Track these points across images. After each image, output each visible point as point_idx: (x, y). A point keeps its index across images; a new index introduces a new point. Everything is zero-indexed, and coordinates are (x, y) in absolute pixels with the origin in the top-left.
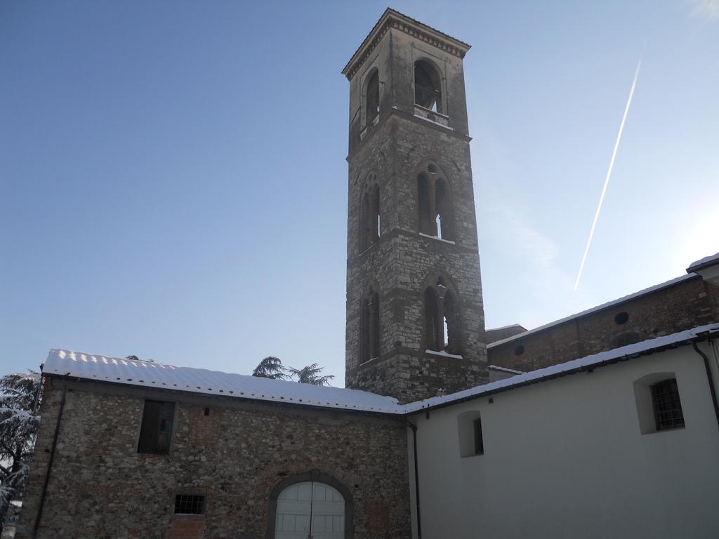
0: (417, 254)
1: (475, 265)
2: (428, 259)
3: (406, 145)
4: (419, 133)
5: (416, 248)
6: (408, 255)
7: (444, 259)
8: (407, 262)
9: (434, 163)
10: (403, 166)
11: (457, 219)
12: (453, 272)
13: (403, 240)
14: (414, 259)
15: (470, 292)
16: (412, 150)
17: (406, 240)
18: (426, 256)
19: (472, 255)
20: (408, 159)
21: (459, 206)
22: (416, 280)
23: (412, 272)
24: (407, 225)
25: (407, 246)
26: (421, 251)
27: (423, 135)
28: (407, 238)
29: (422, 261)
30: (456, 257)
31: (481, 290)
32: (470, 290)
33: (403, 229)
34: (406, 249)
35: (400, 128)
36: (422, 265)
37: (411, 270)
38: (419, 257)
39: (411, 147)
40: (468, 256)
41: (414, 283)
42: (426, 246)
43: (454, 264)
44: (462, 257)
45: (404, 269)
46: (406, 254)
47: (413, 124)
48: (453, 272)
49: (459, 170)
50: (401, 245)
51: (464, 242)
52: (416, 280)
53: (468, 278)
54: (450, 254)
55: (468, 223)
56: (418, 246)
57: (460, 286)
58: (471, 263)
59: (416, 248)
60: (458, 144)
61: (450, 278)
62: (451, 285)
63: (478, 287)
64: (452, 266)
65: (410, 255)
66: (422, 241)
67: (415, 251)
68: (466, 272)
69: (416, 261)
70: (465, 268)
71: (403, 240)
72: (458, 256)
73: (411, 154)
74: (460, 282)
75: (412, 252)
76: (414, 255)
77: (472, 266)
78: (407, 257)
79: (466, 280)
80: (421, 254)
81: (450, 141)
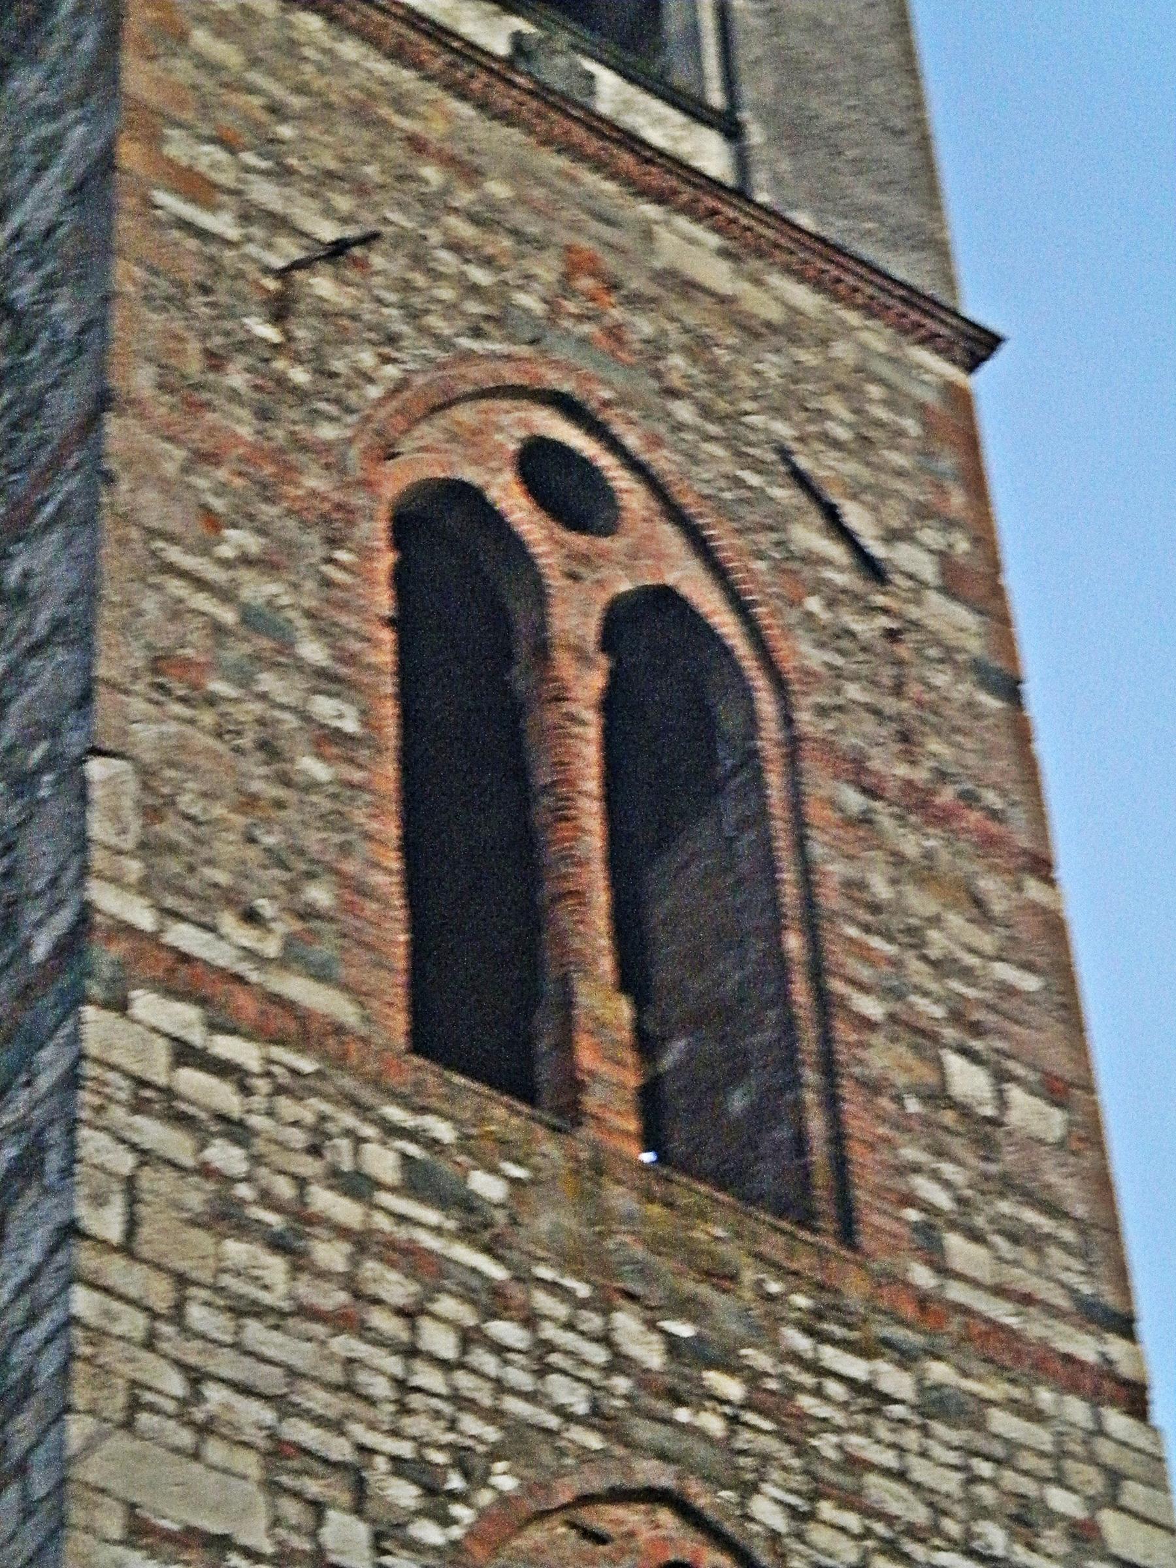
2: (505, 1331)
5: (358, 1185)
6: (244, 1228)
8: (243, 1310)
10: (215, 361)
13: (184, 1054)
16: (337, 250)
17: (223, 1069)
18: (493, 1301)
20: (280, 310)
24: (251, 917)
25: (236, 1130)
29: (443, 1343)
33: (184, 937)
34: (226, 1156)
36: (428, 1377)
37: (283, 1405)
38: (396, 1287)
39: (329, 232)
42: (487, 1186)
43: (853, 1464)
45: (196, 1377)
46: (226, 1218)
47: (350, 49)
50: (150, 1098)
56: (382, 1162)
58: (1060, 1500)
59: (358, 1185)
67: (346, 1211)
69: (341, 1321)
71: (184, 1054)
73: (322, 285)
75: (304, 1218)
76: (330, 1254)
78: (236, 1250)
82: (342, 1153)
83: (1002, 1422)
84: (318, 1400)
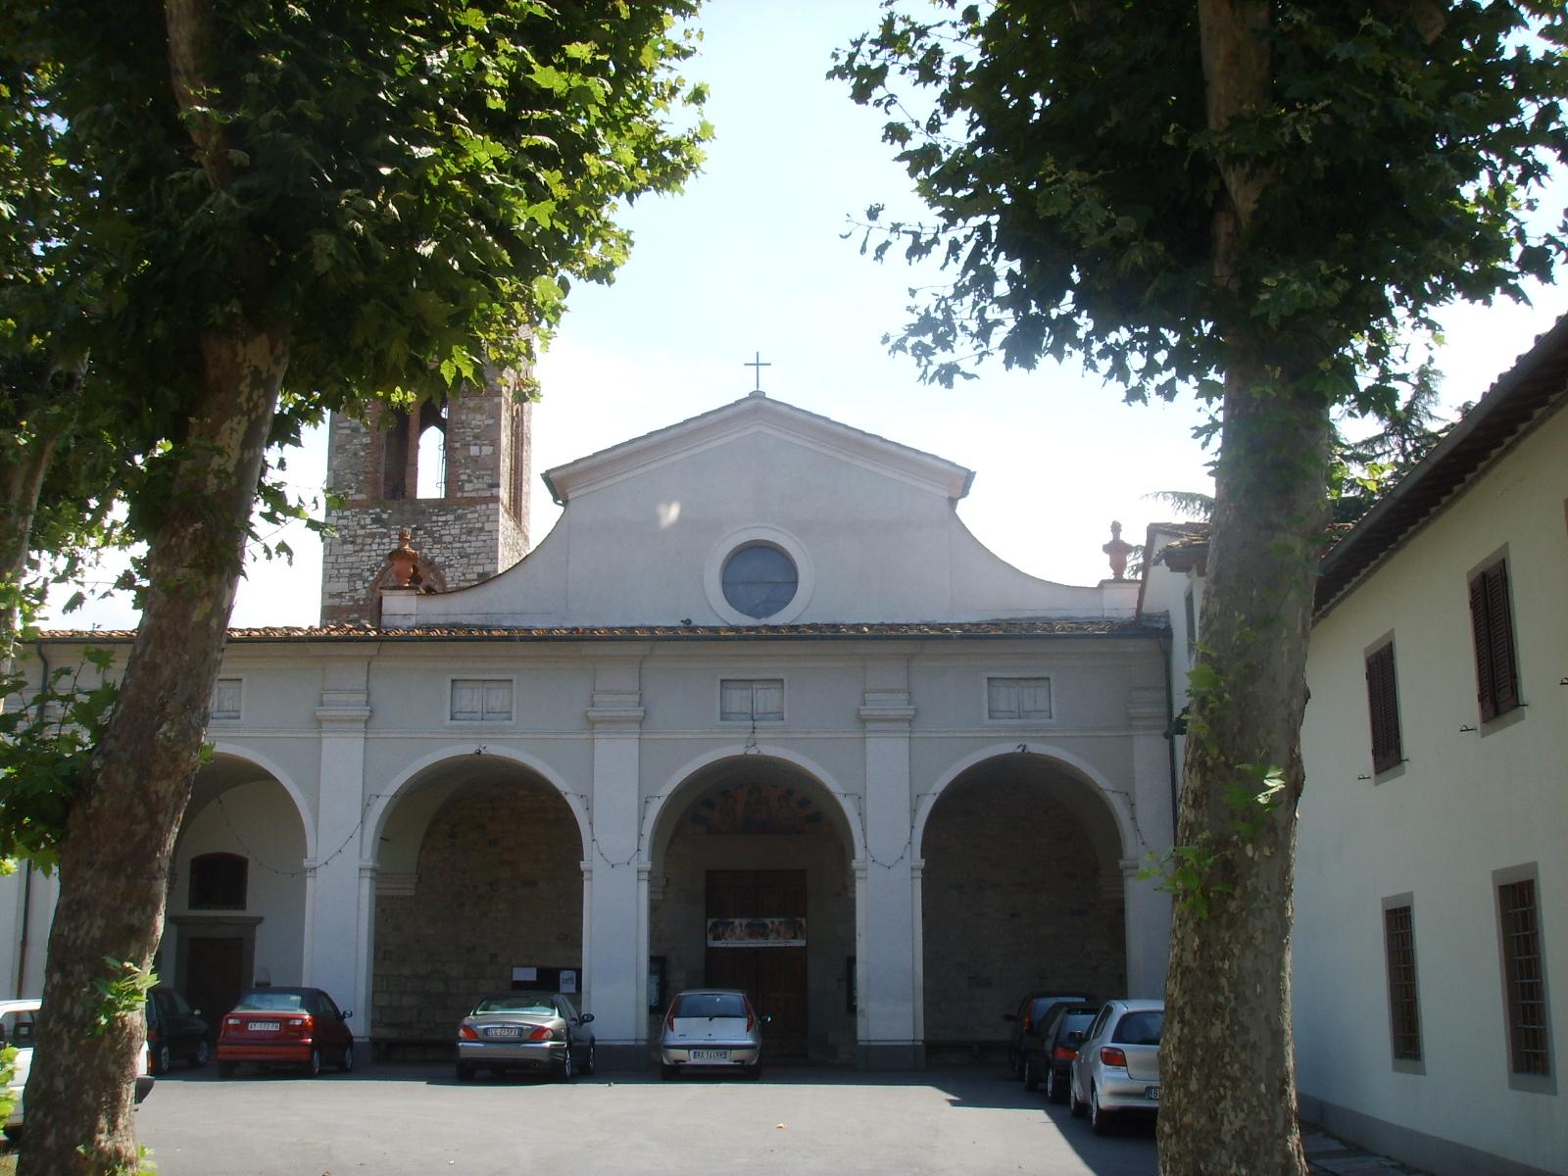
0: (364, 536)
1: (488, 526)
2: (386, 540)
7: (422, 532)
8: (345, 556)
11: (457, 445)
12: (438, 551)
14: (356, 548)
15: (469, 581)
18: (383, 536)
19: (484, 507)
21: (464, 417)
22: (359, 584)
23: (354, 571)
26: (375, 528)
28: (347, 513)
30: (446, 523)
32: (468, 577)
36: (373, 554)
38: (369, 541)
40: (476, 512)
41: (356, 590)
42: (385, 516)
43: (441, 536)
44: (458, 518)
45: (338, 570)
46: (344, 542)
48: (438, 551)
51: (468, 487)
52: (359, 584)
53: (467, 556)
54: (434, 518)
55: (480, 446)
56: (368, 521)
57: (448, 574)
59: (363, 527)
61: (430, 563)
62: (432, 576)
64: (438, 540)
65: (352, 542)
66: (378, 510)
67: (362, 532)
68: (466, 545)
69: (362, 550)
70: (464, 538)
71: (339, 518)
72: (450, 517)
74: (450, 566)
75: (355, 536)
76: (359, 541)
77: (481, 529)
78: (345, 547)
79: (465, 560)
80: (373, 536)
82: (362, 523)
83: (469, 516)
84: (356, 565)
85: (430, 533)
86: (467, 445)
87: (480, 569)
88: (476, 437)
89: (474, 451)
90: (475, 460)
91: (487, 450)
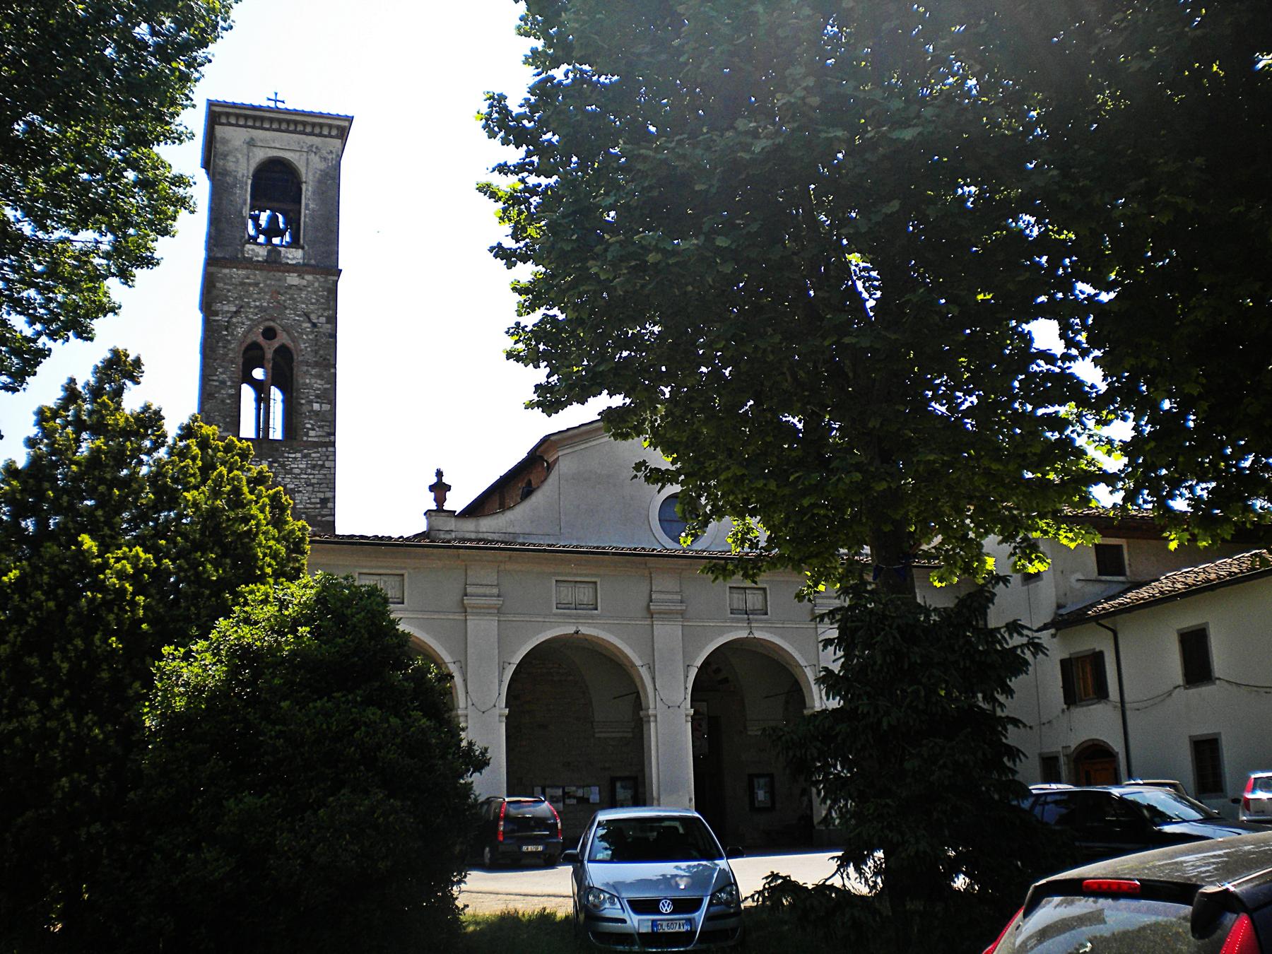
1: (327, 464)
3: (226, 308)
4: (250, 284)
9: (272, 324)
16: (236, 313)
27: (257, 285)
30: (295, 458)
31: (334, 497)
35: (220, 285)
39: (234, 309)
44: (305, 456)
49: (314, 325)
51: (312, 433)
53: (312, 485)
60: (316, 284)
63: (329, 495)
64: (290, 472)
72: (299, 455)
73: (234, 320)
77: (323, 466)
79: (310, 488)
81: (305, 283)
85: (283, 466)
86: (311, 402)
87: (322, 495)
88: (317, 396)
89: (316, 406)
90: (317, 413)
91: (326, 407)
